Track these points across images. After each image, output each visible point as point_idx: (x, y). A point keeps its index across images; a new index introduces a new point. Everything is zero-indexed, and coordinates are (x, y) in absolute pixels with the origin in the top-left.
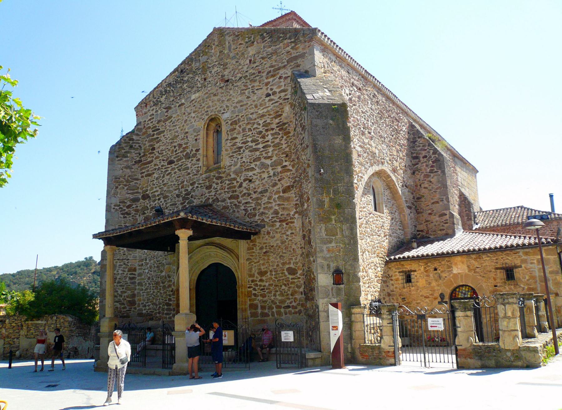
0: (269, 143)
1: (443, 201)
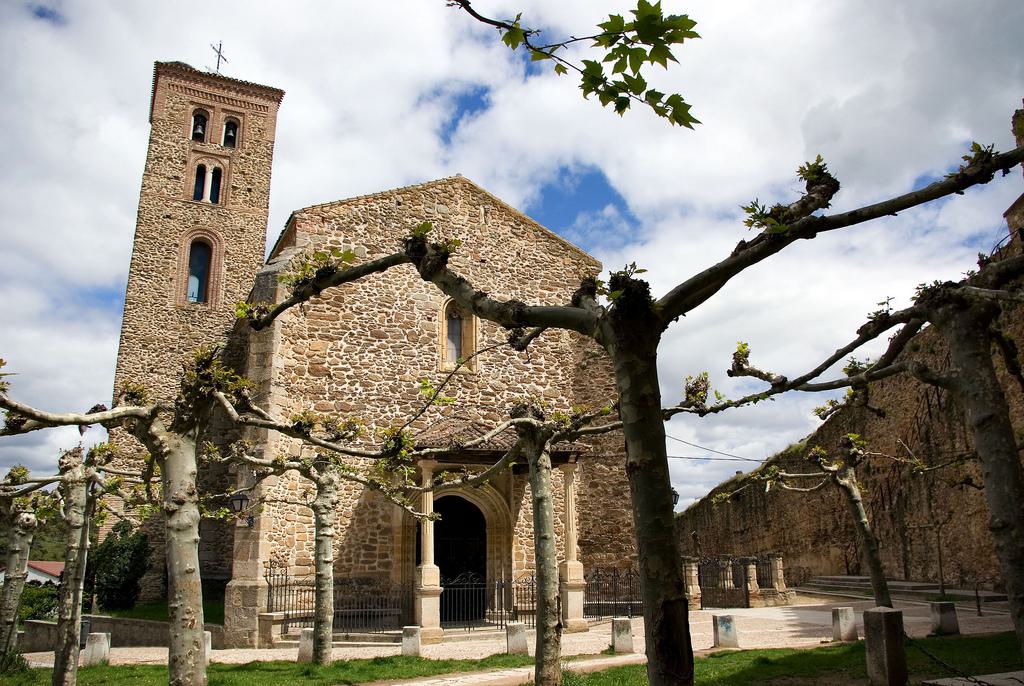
0: (543, 367)
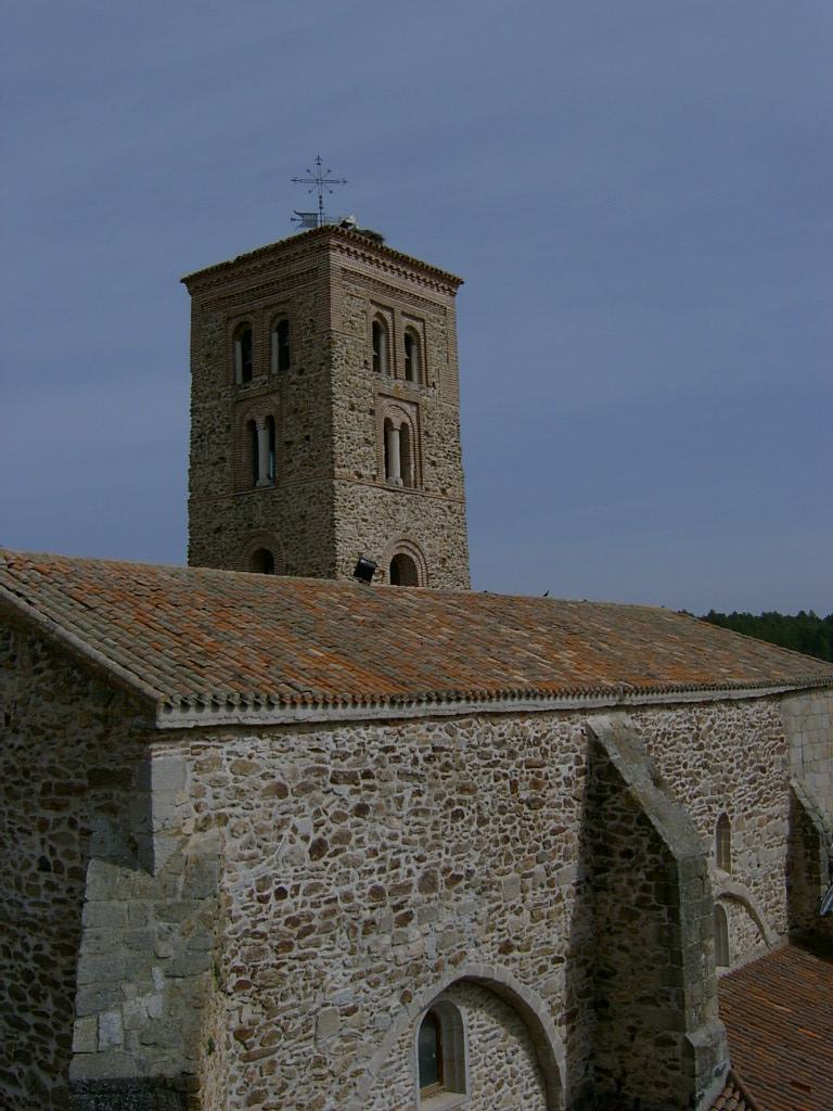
1: (669, 1000)
